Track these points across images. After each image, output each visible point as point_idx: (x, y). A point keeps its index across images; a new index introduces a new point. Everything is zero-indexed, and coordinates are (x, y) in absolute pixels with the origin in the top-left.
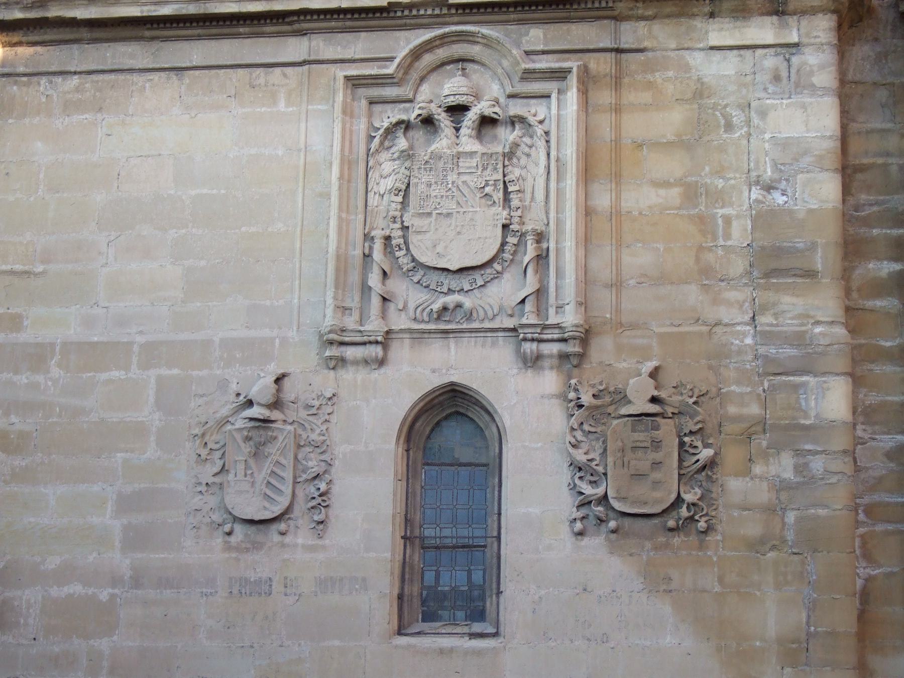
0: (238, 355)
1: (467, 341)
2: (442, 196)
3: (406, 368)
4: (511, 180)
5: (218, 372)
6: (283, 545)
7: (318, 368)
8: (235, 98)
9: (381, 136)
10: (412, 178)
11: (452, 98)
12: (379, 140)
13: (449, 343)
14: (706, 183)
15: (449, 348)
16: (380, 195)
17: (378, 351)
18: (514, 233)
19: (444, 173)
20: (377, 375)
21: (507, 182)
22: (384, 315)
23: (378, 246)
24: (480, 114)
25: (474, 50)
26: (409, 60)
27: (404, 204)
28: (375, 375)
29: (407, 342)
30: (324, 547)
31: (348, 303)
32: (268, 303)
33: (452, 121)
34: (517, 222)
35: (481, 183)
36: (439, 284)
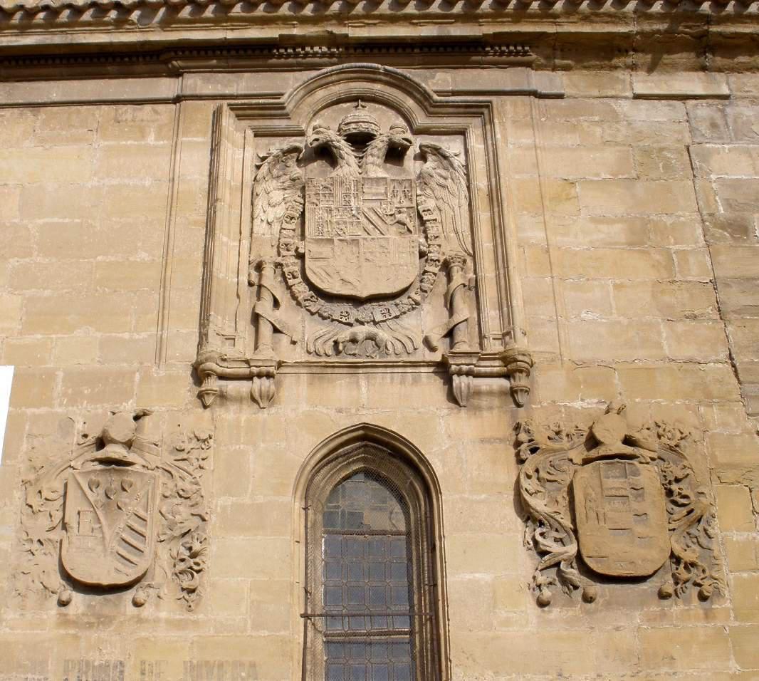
0: (86, 392)
4: (426, 209)
5: (60, 410)
6: (140, 620)
7: (189, 406)
8: (97, 132)
13: (358, 380)
14: (653, 220)
20: (266, 415)
28: (264, 415)
29: (304, 378)
30: (196, 623)
32: (126, 336)
35: (391, 210)
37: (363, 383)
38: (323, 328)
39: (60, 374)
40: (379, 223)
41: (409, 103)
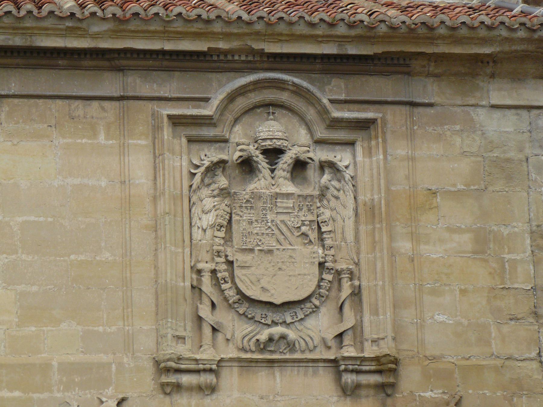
1: (291, 372)
2: (263, 234)
3: (236, 394)
4: (324, 221)
7: (154, 393)
9: (202, 174)
10: (233, 215)
11: (268, 143)
12: (200, 178)
13: (274, 372)
15: (274, 377)
16: (203, 229)
17: (210, 378)
18: (328, 271)
19: (264, 212)
20: (209, 401)
21: (320, 222)
22: (214, 346)
23: (206, 279)
24: (295, 158)
25: (284, 97)
26: (225, 103)
27: (228, 239)
29: (236, 370)
31: (181, 333)
32: (101, 329)
33: (267, 163)
34: (331, 261)
35: (297, 223)
36: (263, 316)
37: (278, 374)
38: (248, 328)
39: (55, 363)
40: (288, 234)
41: (311, 114)
